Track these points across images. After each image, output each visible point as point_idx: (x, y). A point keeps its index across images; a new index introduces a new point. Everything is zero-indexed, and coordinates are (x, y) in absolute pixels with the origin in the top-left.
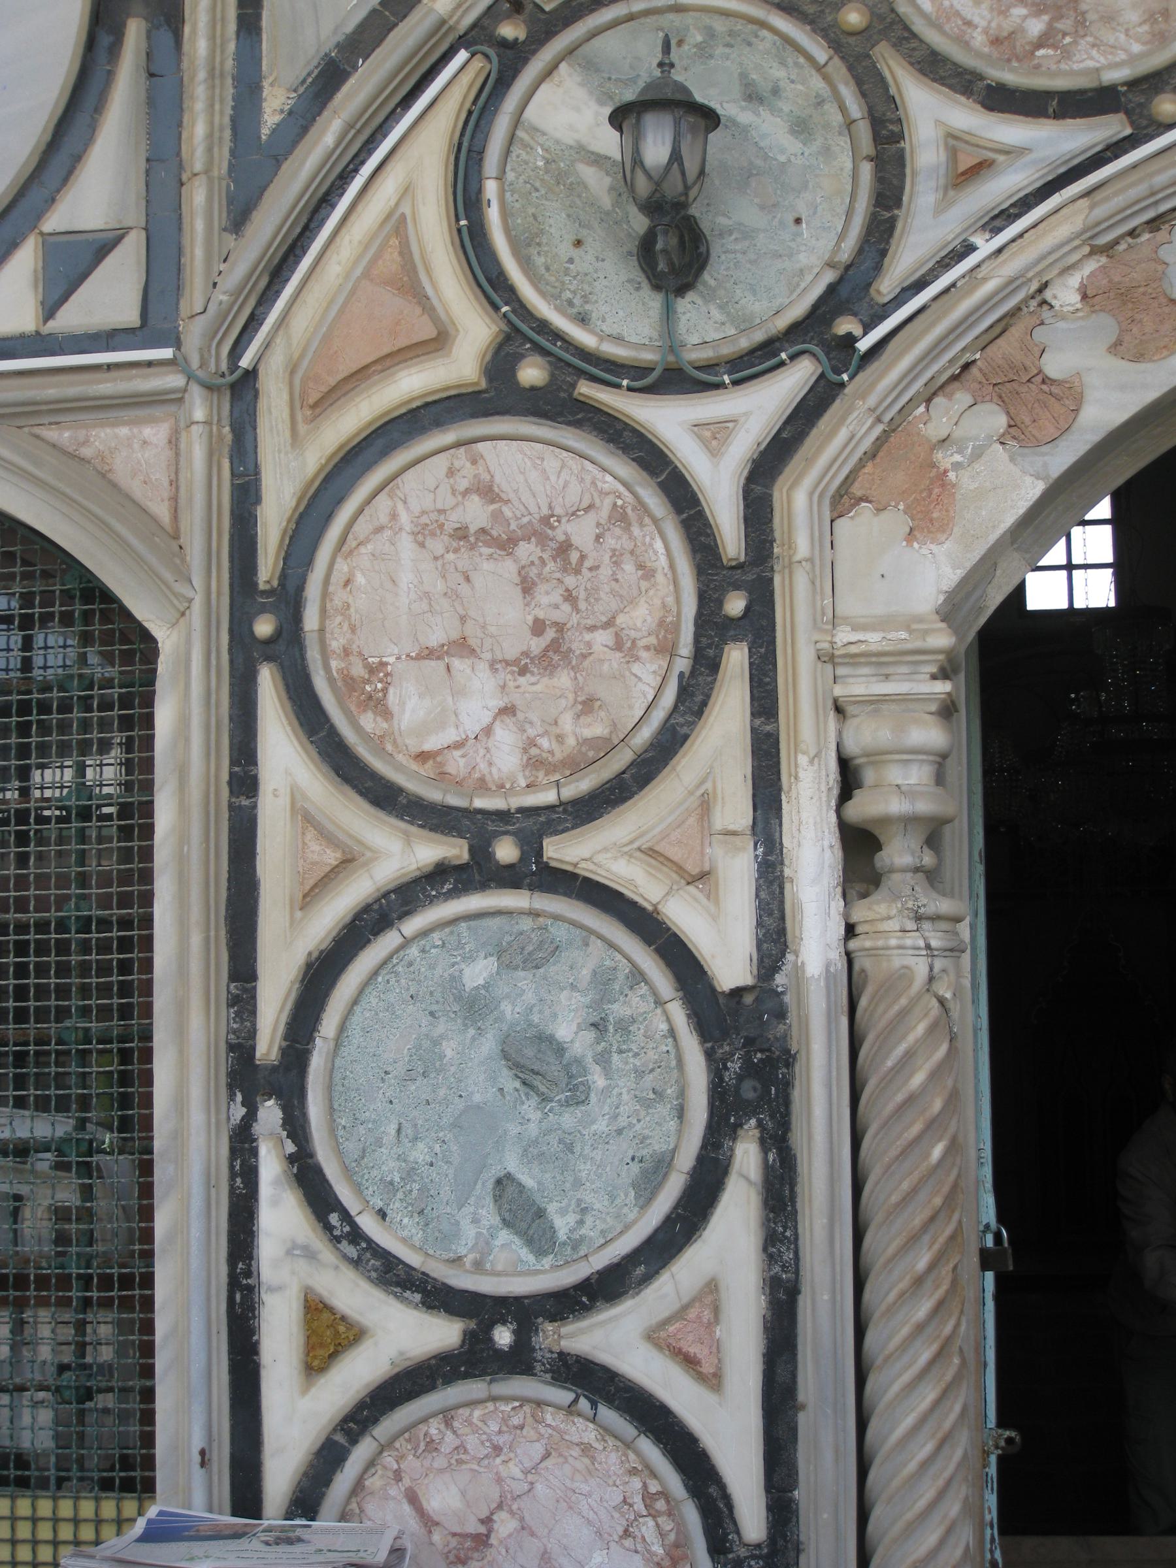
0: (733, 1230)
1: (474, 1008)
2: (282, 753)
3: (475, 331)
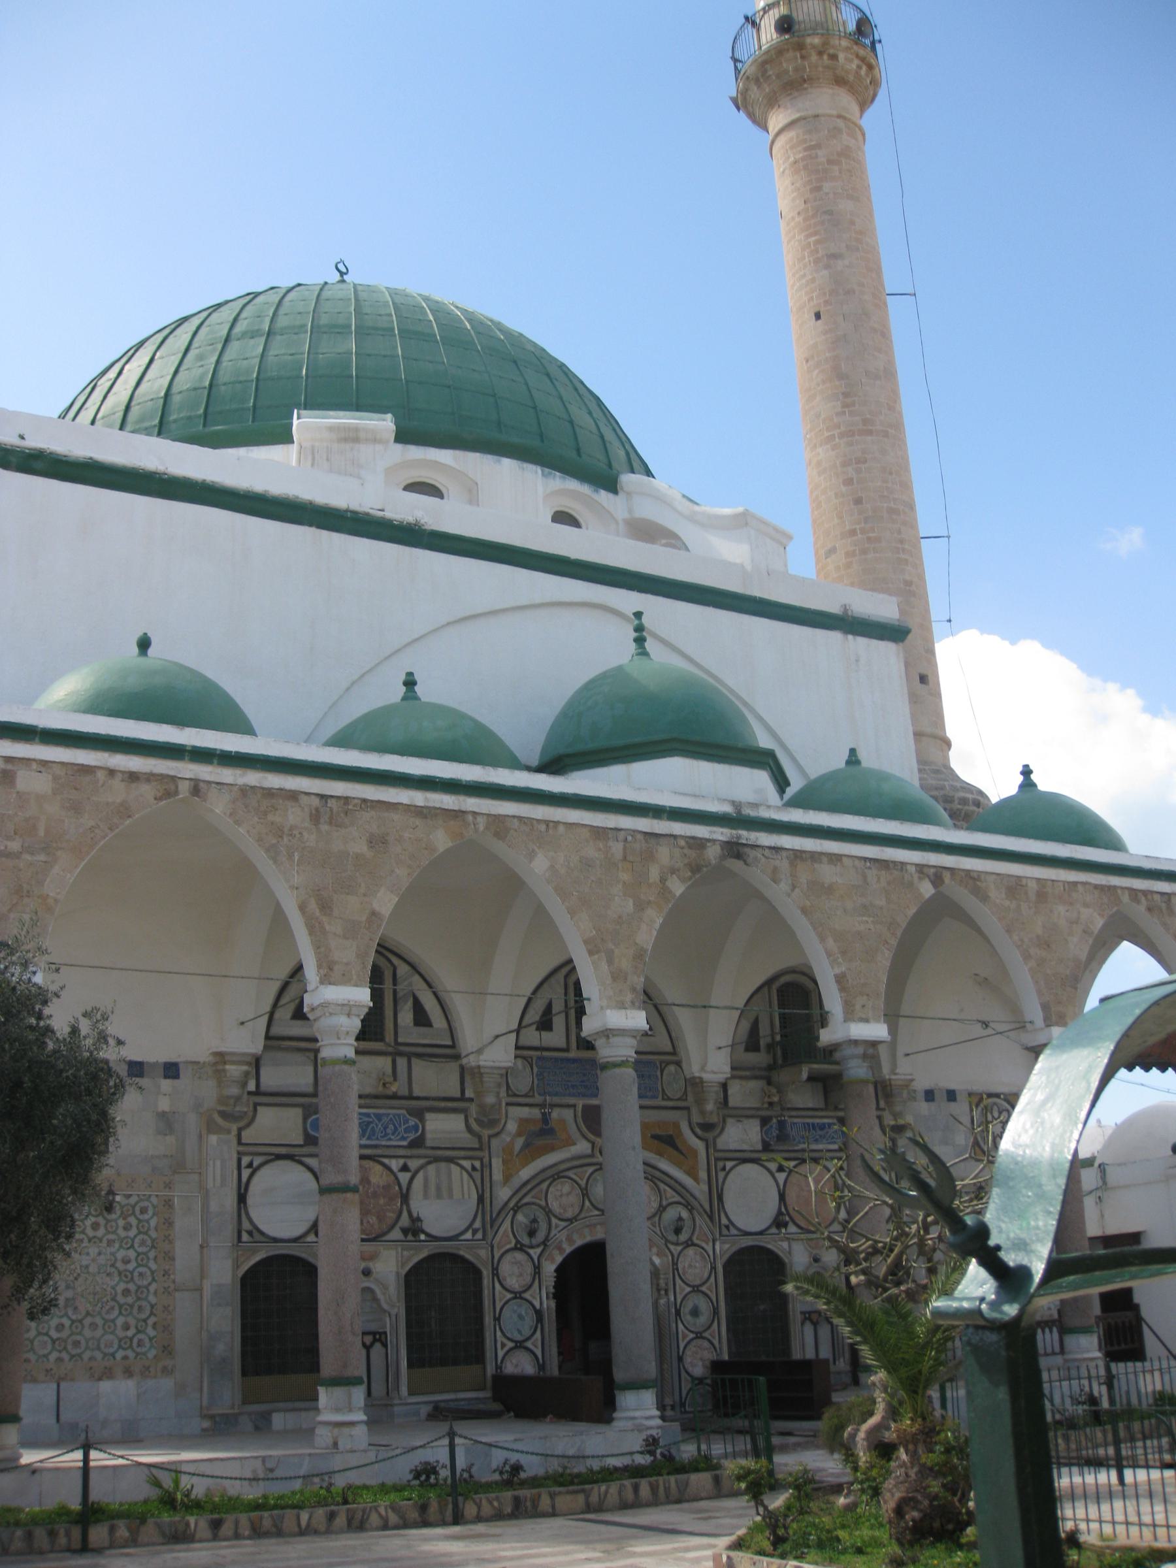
0: (538, 1334)
1: (515, 1312)
2: (497, 1285)
3: (514, 1241)
